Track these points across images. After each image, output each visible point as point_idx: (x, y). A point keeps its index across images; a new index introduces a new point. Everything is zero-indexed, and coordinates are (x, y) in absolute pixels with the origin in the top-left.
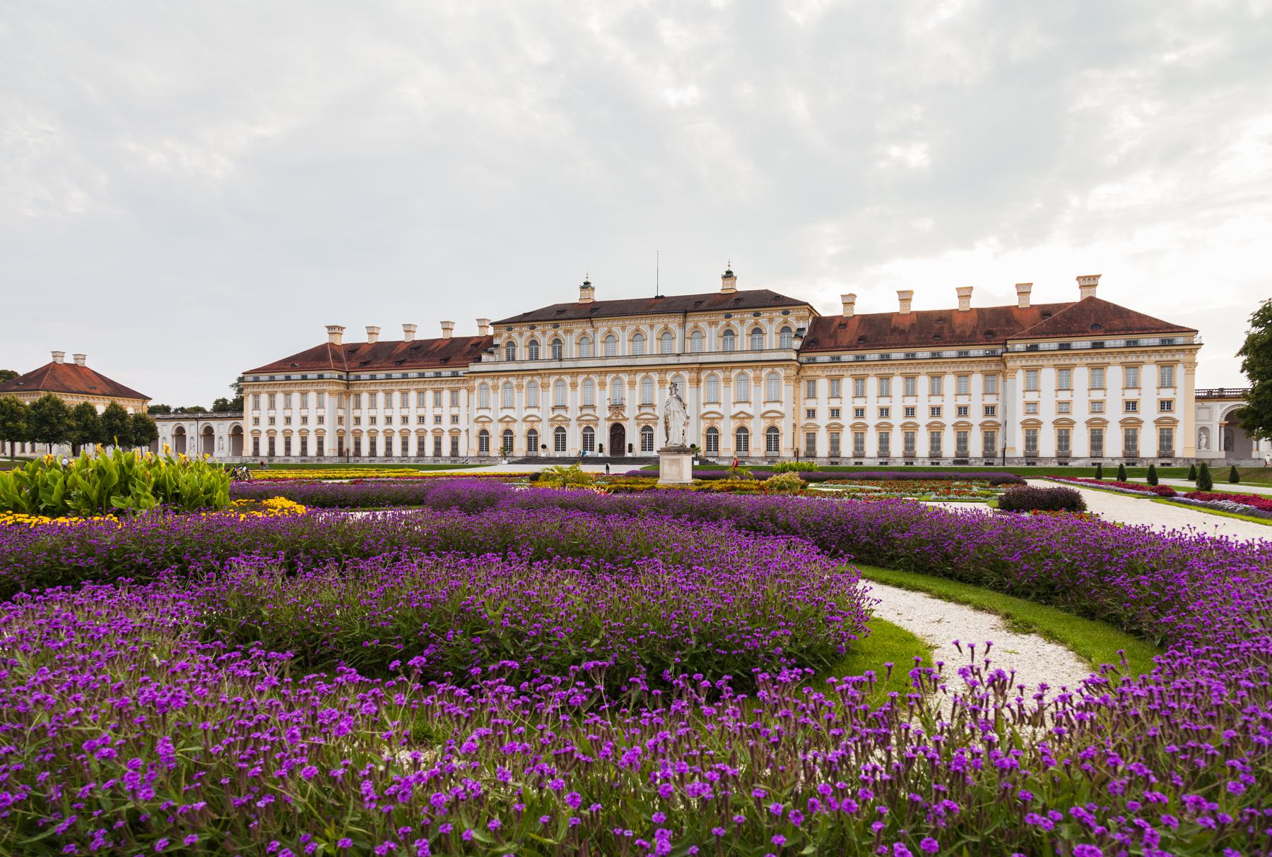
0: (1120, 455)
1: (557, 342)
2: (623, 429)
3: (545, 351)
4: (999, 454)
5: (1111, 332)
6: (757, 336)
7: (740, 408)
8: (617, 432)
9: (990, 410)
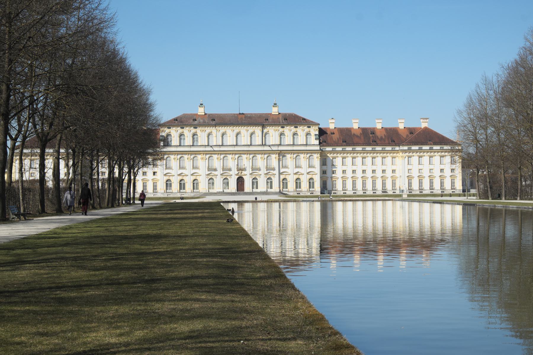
2: (243, 179)
3: (188, 141)
5: (436, 144)
8: (240, 181)
9: (394, 171)
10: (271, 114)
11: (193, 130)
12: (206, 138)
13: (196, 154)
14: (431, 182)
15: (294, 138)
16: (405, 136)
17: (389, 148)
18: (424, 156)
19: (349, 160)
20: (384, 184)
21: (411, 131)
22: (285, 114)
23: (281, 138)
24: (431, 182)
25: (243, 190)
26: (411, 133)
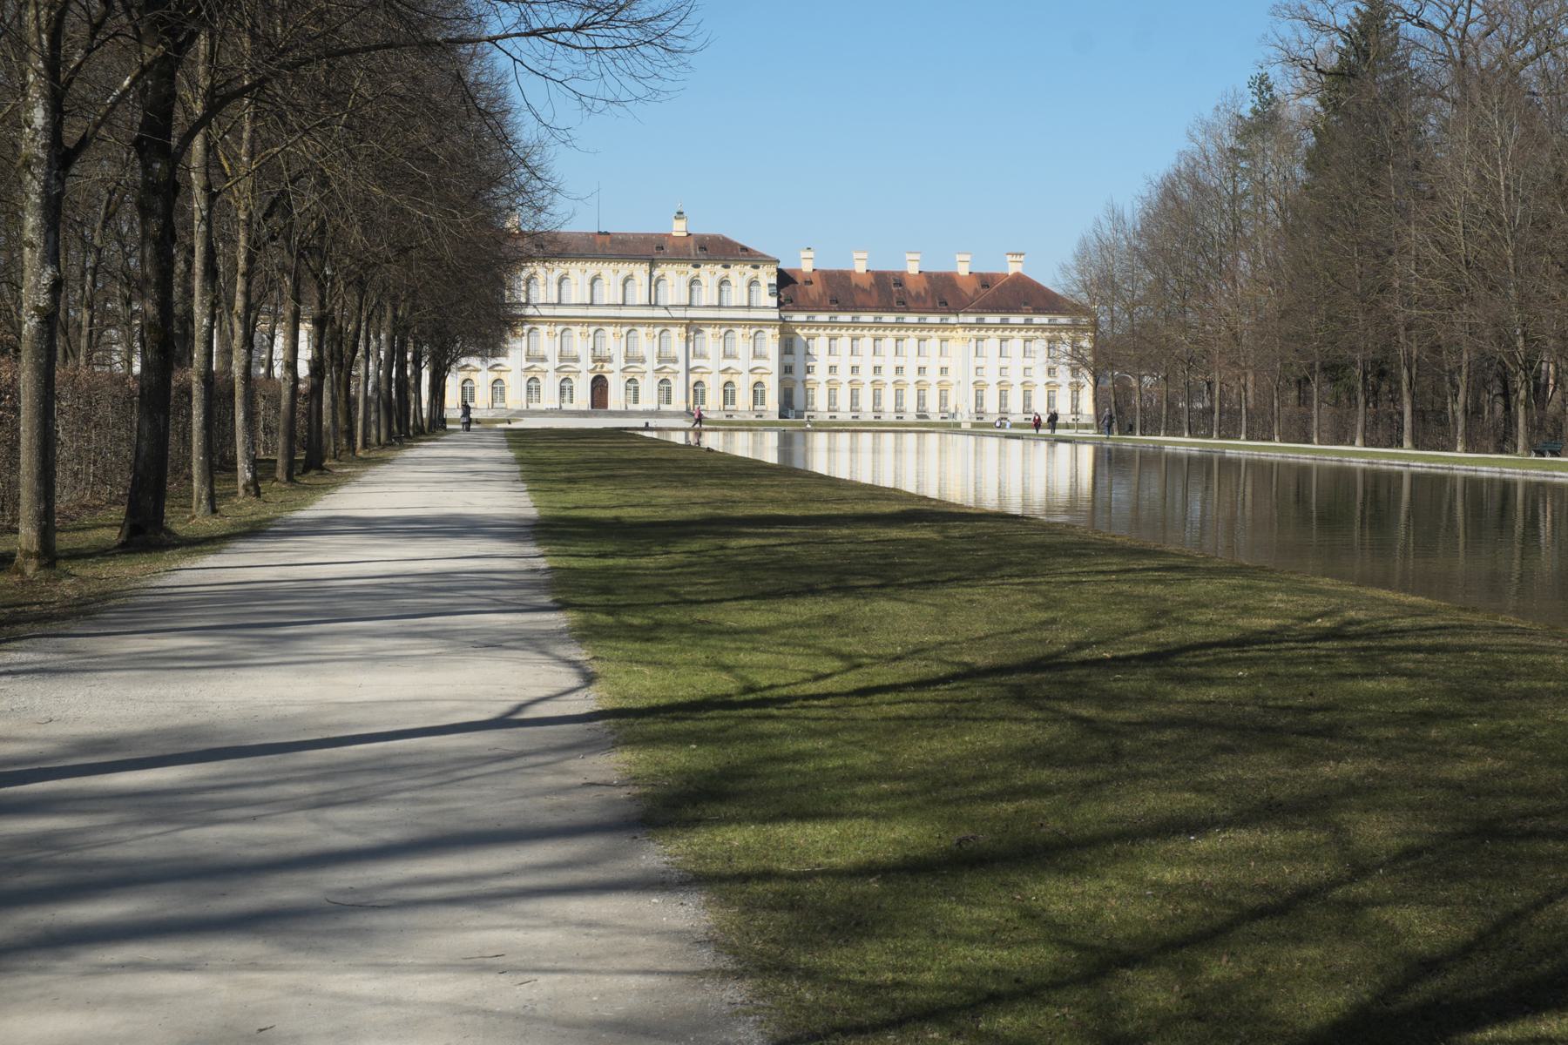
5: (1039, 311)
6: (725, 288)
7: (726, 363)
8: (599, 386)
9: (944, 370)
10: (669, 235)
16: (970, 292)
17: (934, 319)
19: (844, 343)
20: (921, 399)
21: (985, 281)
22: (702, 237)
23: (691, 290)
25: (605, 405)
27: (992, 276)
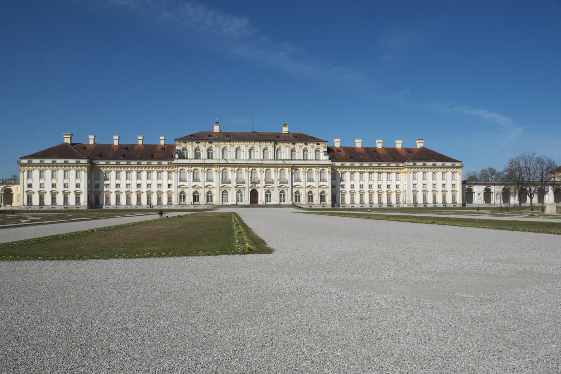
0: (441, 202)
1: (209, 150)
3: (203, 154)
4: (402, 203)
5: (438, 160)
6: (305, 153)
8: (254, 194)
9: (398, 186)
11: (208, 145)
12: (221, 153)
13: (210, 166)
14: (434, 197)
15: (304, 154)
16: (405, 155)
17: (393, 165)
18: (428, 172)
20: (389, 198)
21: (409, 151)
23: (292, 154)
24: (434, 197)
25: (257, 202)
26: (409, 152)
27: (411, 149)
